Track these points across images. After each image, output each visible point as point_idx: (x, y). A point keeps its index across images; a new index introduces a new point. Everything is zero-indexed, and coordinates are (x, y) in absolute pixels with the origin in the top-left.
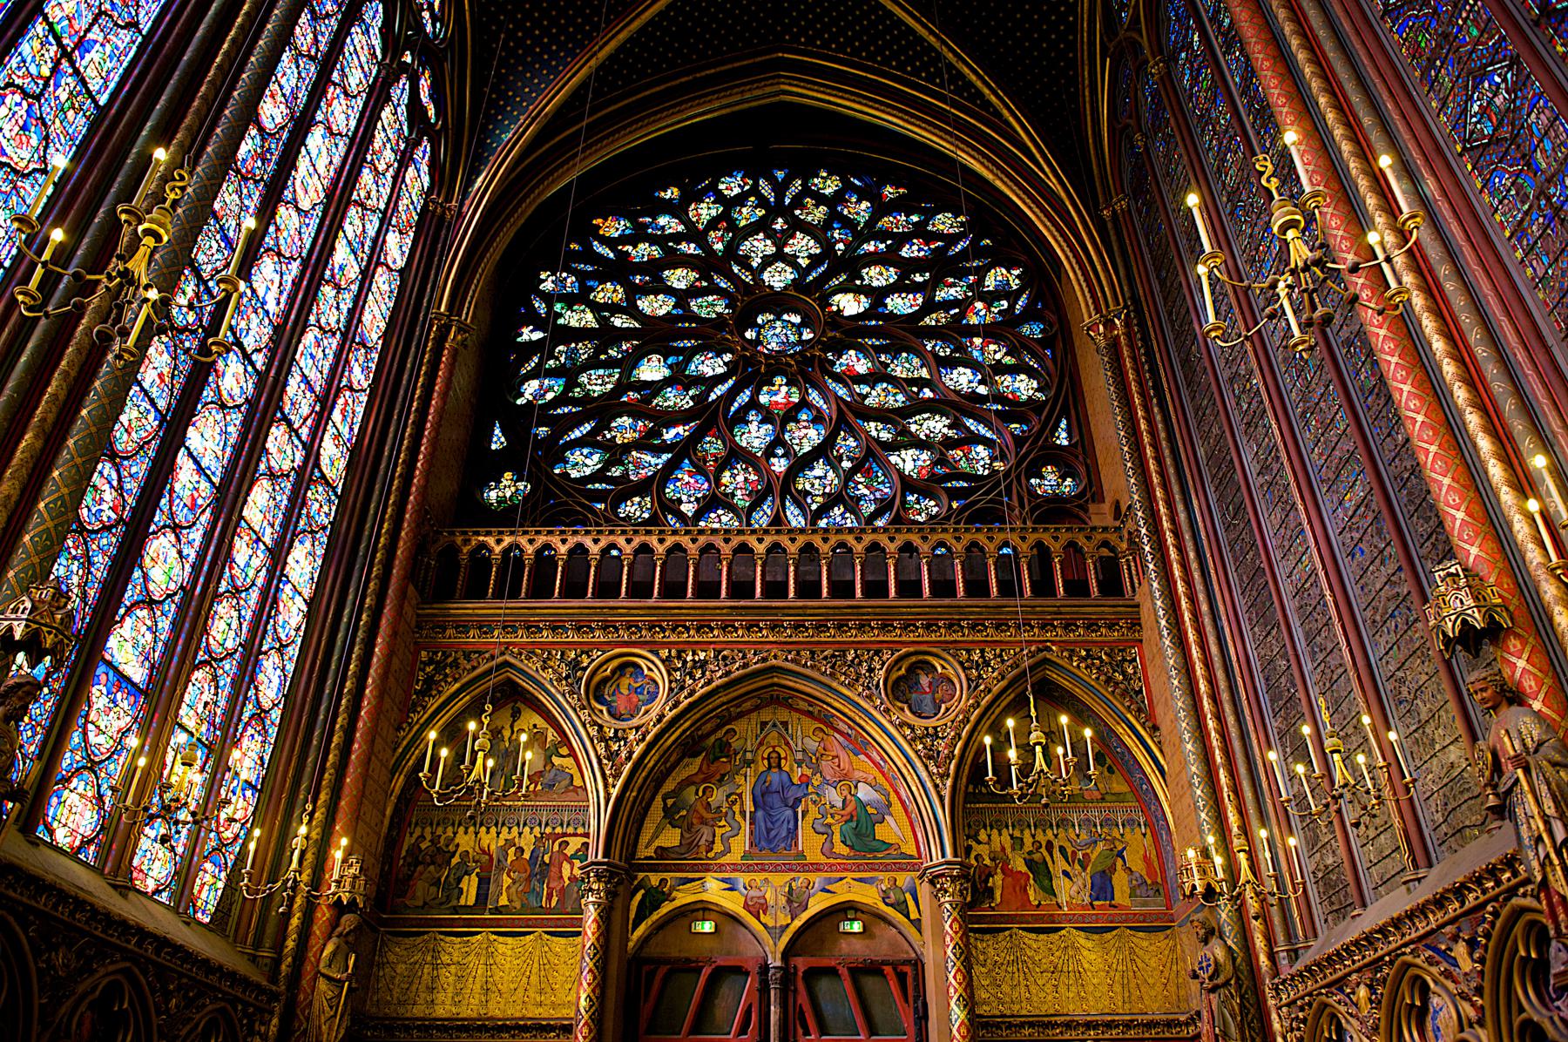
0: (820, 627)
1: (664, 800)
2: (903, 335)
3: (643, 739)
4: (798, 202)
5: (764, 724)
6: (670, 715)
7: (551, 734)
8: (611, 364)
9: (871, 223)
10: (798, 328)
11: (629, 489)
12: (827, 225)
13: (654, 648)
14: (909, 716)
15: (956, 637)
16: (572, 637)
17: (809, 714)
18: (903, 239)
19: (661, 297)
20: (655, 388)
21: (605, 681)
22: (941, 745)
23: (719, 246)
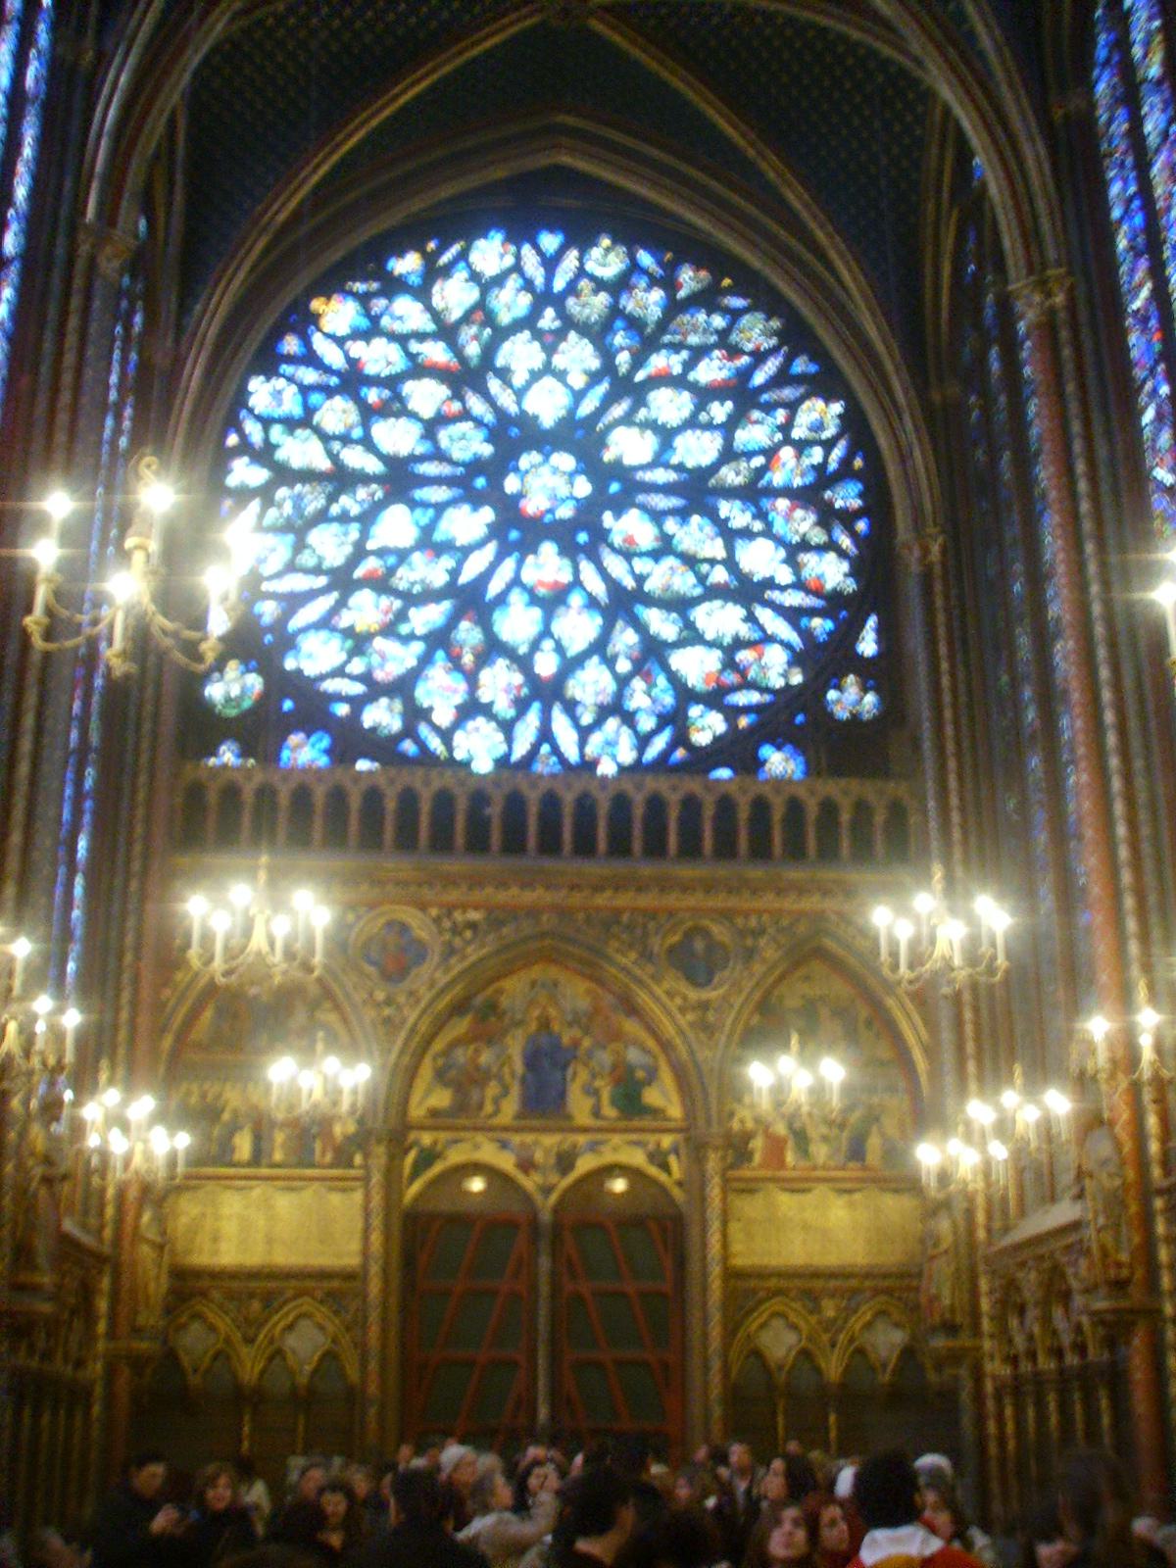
0: (598, 888)
1: (434, 1059)
2: (697, 492)
3: (418, 1001)
8: (344, 518)
9: (663, 325)
10: (572, 475)
11: (375, 690)
13: (423, 907)
14: (683, 987)
15: (733, 902)
17: (583, 975)
18: (699, 353)
19: (403, 420)
22: (711, 1016)
23: (473, 350)
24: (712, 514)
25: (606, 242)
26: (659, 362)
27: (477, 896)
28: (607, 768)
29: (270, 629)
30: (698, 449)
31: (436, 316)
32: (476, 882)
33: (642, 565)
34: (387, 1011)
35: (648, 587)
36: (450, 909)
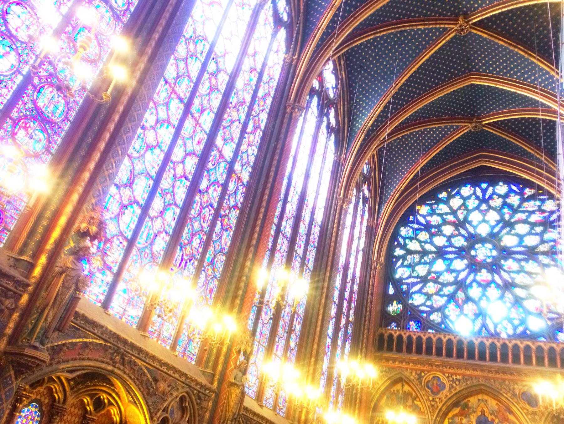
0: (497, 372)
1: (449, 419)
4: (491, 197)
5: (479, 400)
6: (449, 396)
7: (414, 393)
8: (425, 263)
9: (520, 206)
11: (433, 310)
12: (502, 207)
13: (444, 373)
14: (528, 407)
16: (419, 367)
19: (441, 237)
20: (439, 274)
21: (429, 381)
23: (461, 217)
24: (536, 260)
25: (501, 184)
26: (519, 216)
27: (459, 371)
28: (504, 335)
29: (405, 293)
30: (531, 241)
31: (451, 208)
32: (459, 367)
33: (513, 275)
34: (433, 403)
35: (516, 281)
36: (452, 374)
